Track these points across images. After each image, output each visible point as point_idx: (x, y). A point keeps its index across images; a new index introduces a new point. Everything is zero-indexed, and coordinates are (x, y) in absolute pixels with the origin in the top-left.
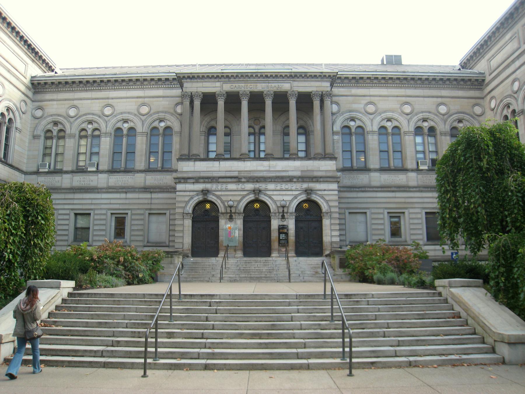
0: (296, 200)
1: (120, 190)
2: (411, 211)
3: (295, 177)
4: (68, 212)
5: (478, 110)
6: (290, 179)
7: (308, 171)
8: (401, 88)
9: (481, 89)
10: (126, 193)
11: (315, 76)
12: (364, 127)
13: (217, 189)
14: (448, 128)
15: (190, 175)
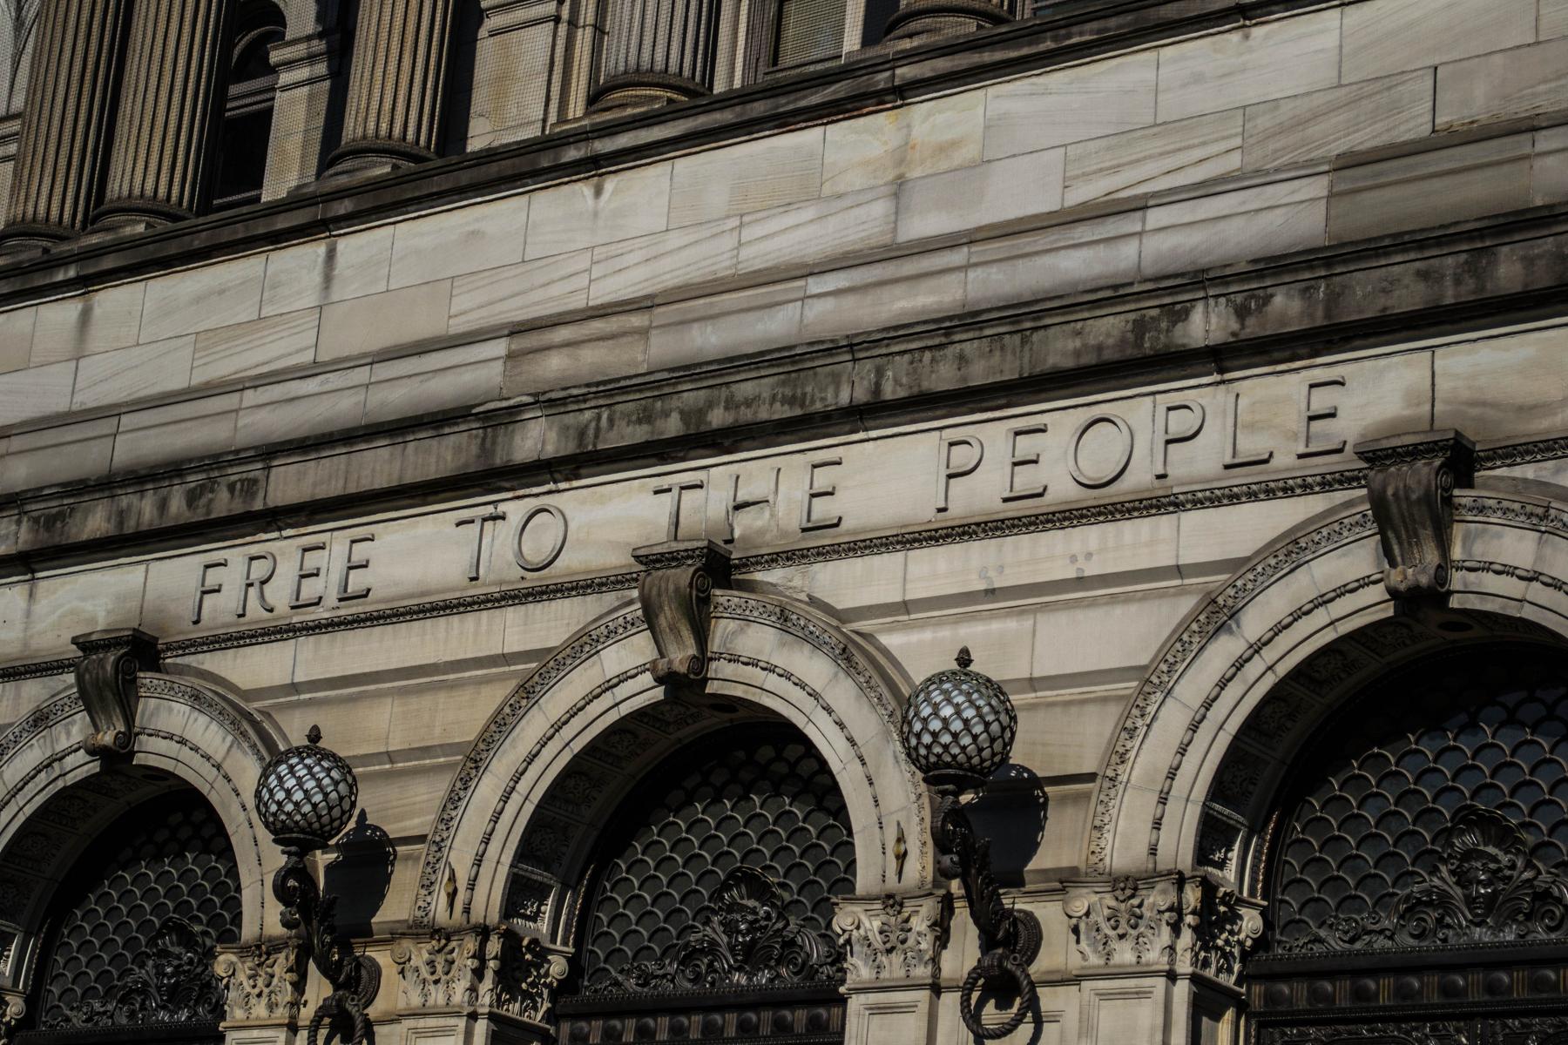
6: (1141, 343)
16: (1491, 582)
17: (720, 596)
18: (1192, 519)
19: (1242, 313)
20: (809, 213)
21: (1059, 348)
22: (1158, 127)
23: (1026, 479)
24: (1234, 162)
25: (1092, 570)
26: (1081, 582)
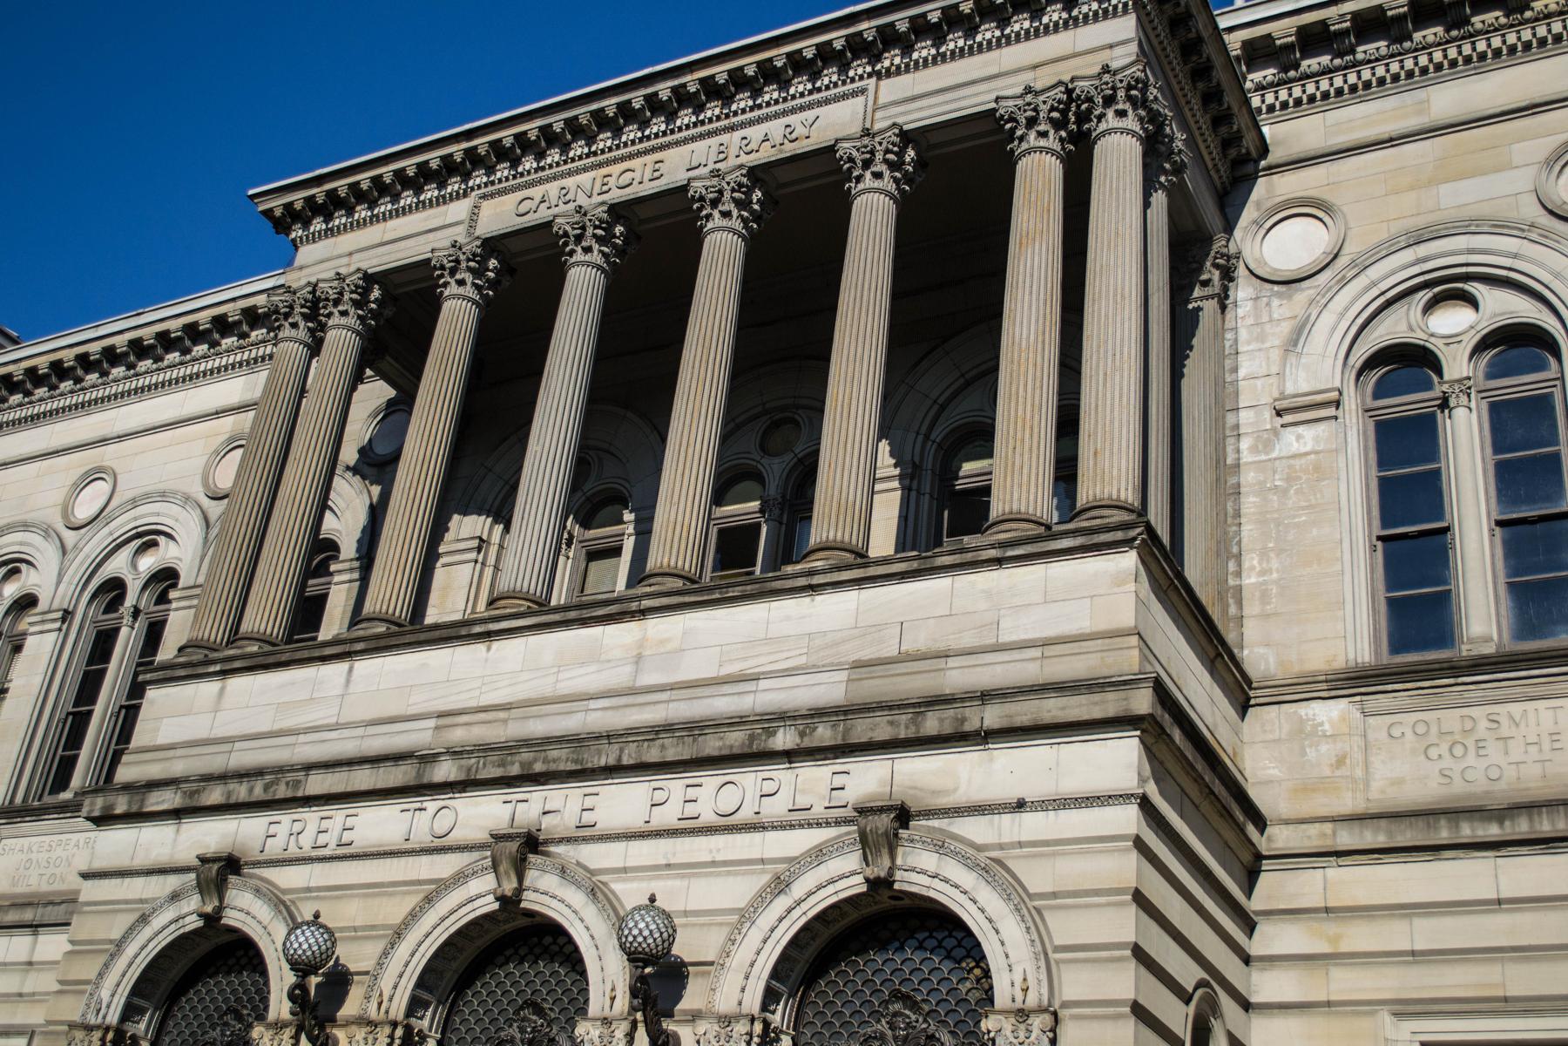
0: (782, 903)
6: (750, 747)
13: (293, 851)
16: (913, 877)
17: (532, 858)
18: (771, 835)
19: (802, 735)
20: (593, 668)
21: (712, 745)
22: (768, 640)
23: (691, 810)
24: (802, 660)
25: (719, 858)
26: (714, 863)
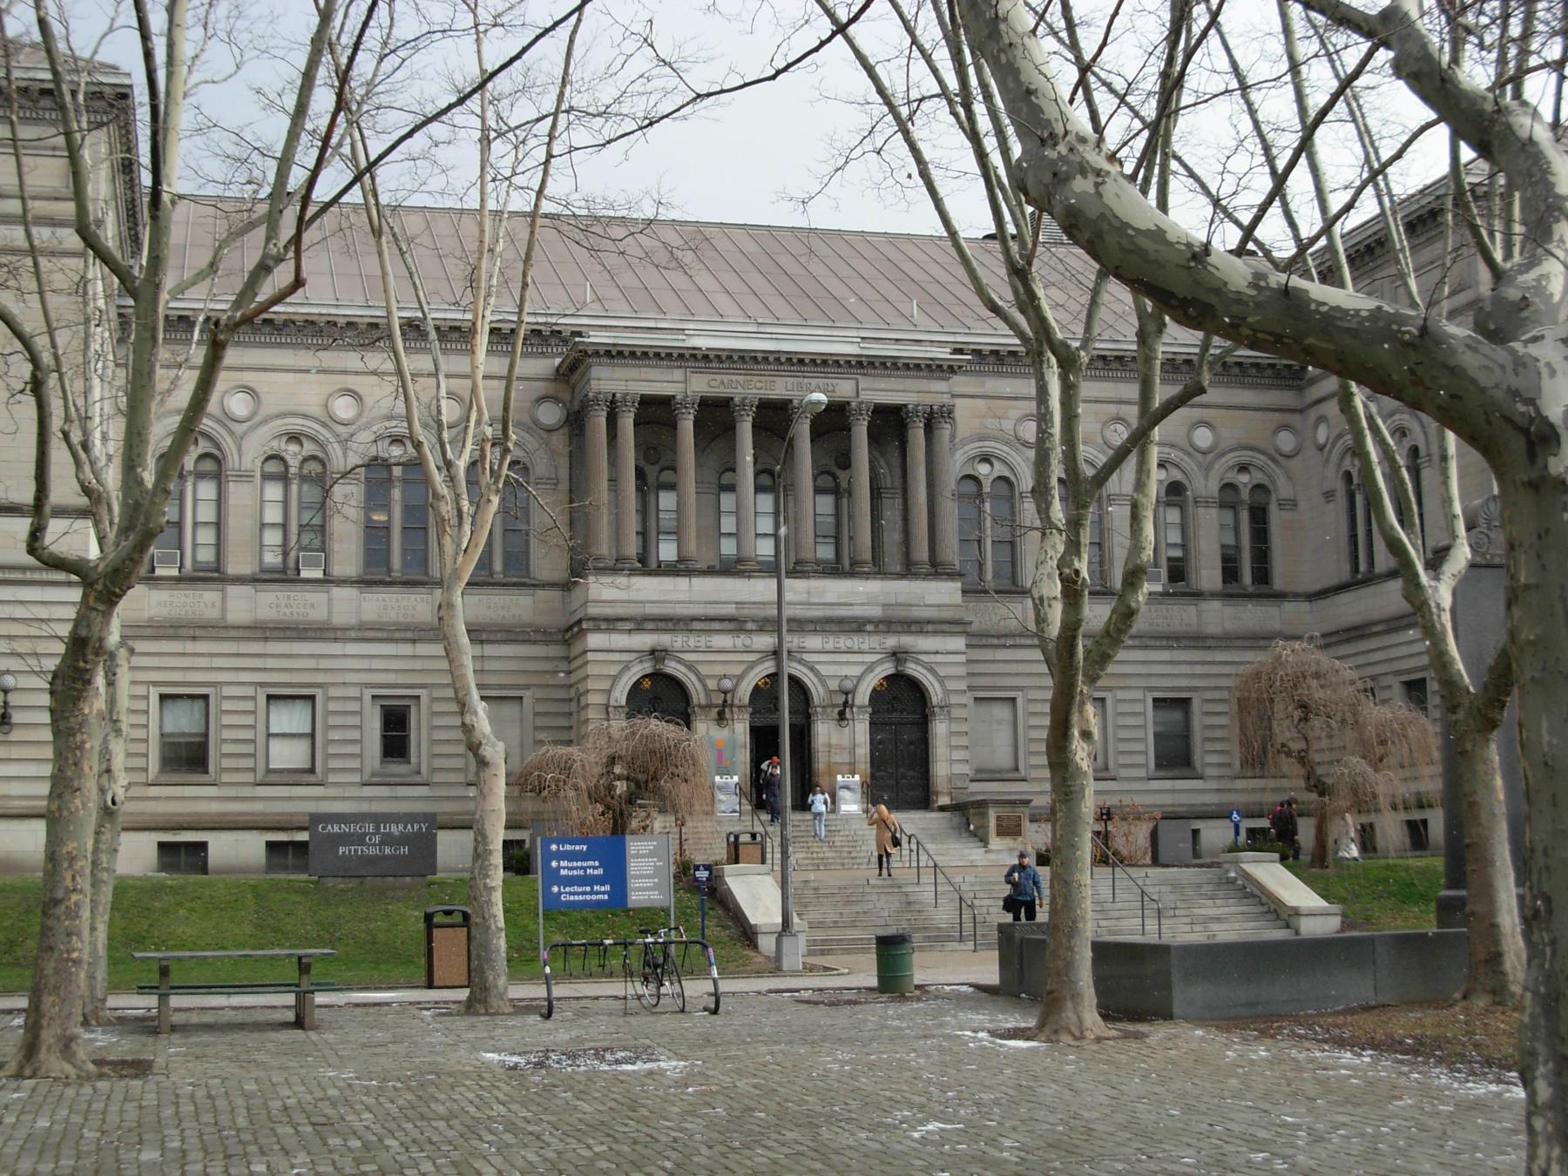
1: (397, 635)
2: (1121, 695)
3: (870, 621)
4: (250, 691)
5: (1286, 441)
6: (857, 626)
7: (897, 604)
8: (1106, 379)
9: (1300, 389)
10: (414, 641)
11: (918, 366)
12: (1013, 478)
14: (1213, 487)
15: (620, 611)
